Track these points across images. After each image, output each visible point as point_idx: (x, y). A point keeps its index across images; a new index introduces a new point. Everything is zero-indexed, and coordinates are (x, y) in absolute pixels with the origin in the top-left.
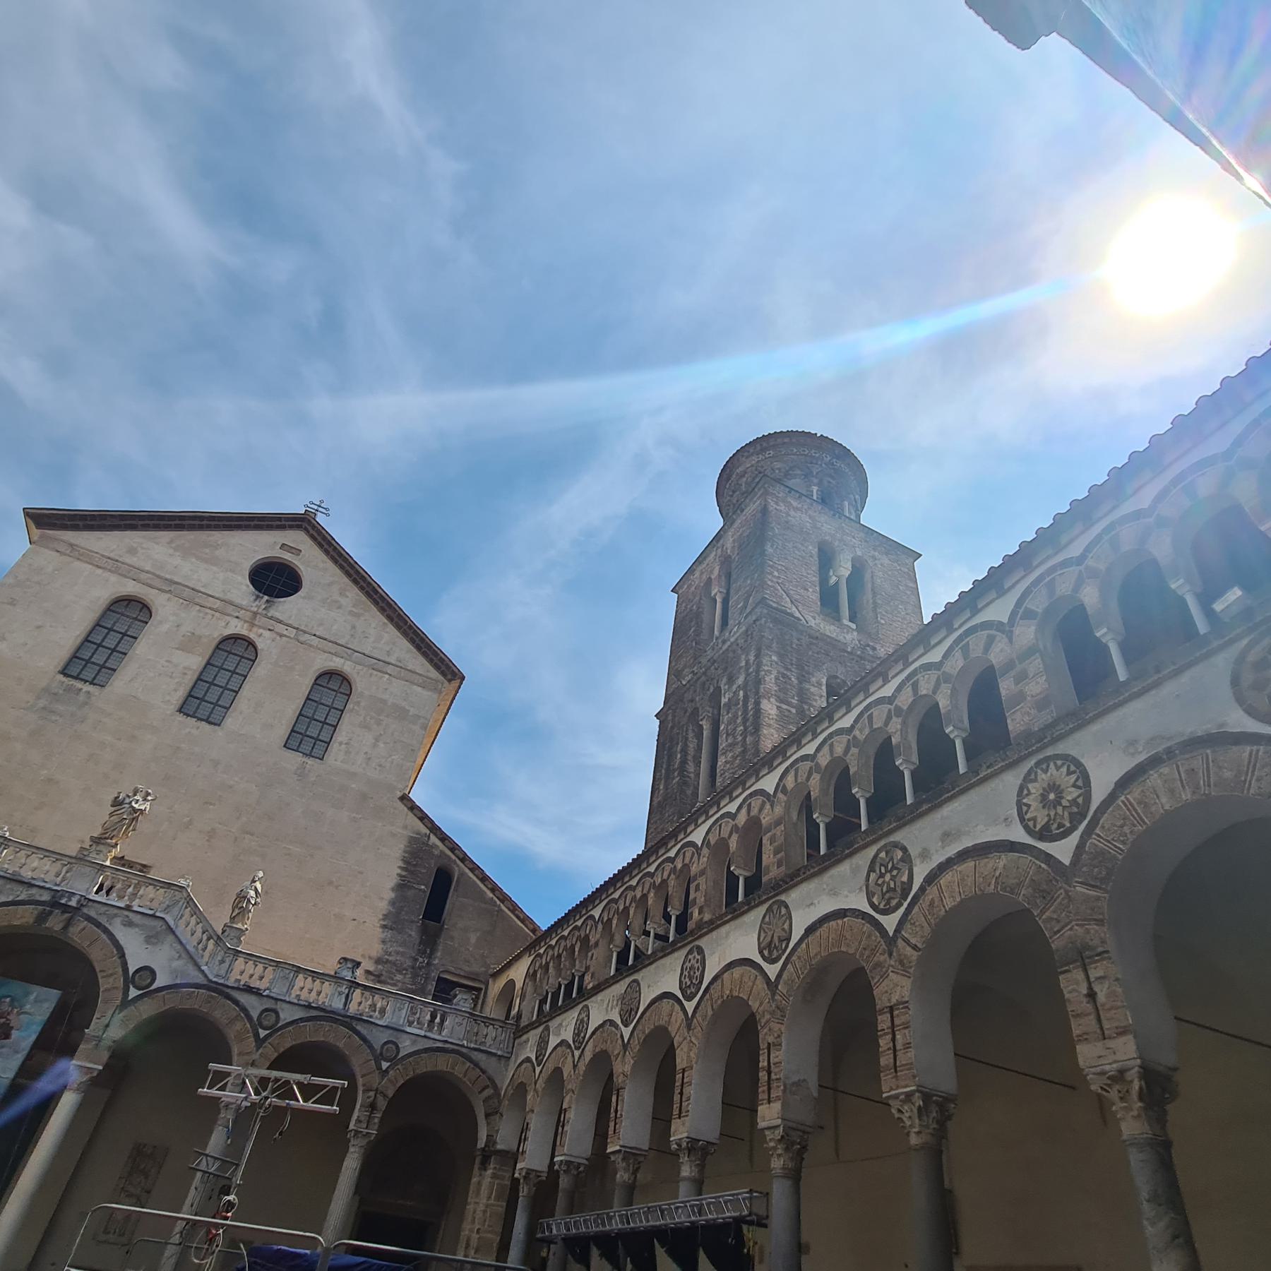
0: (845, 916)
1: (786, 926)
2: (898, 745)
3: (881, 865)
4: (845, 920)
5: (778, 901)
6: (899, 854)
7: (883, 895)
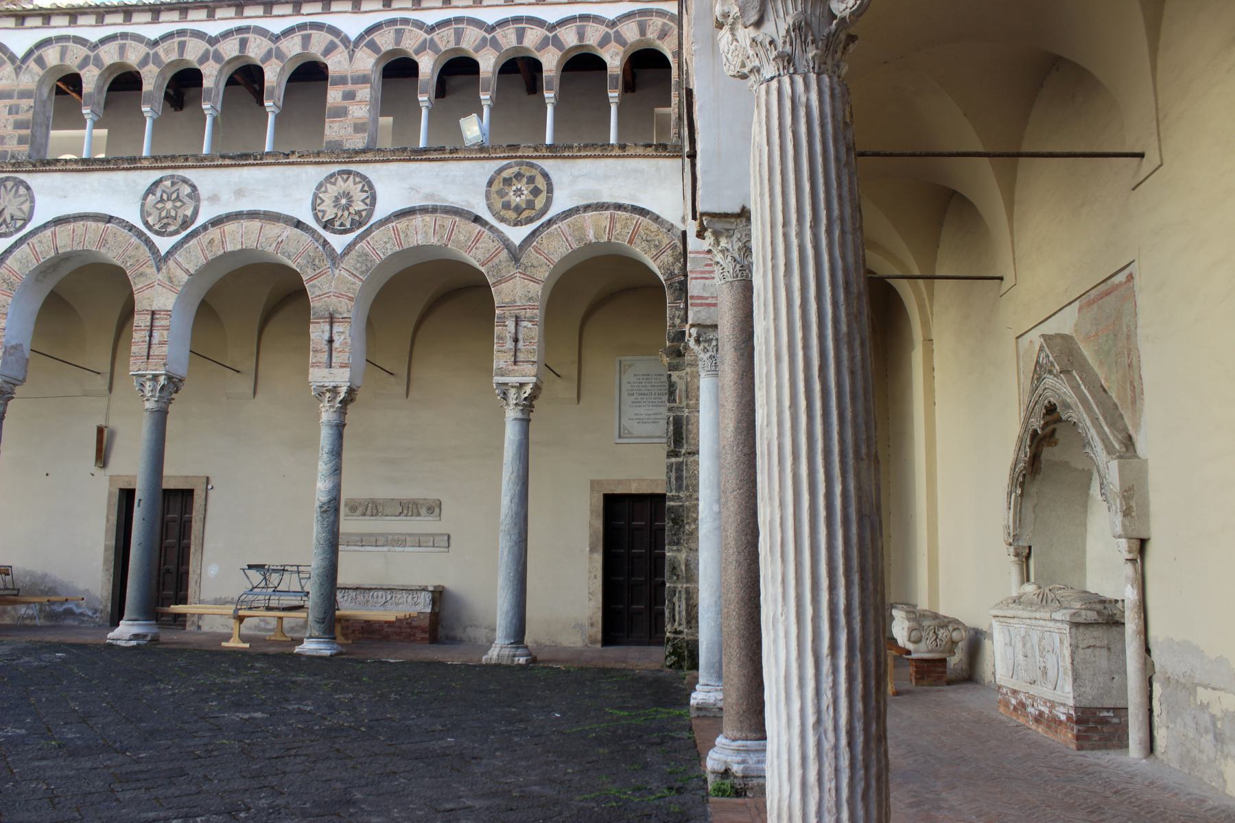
0: (109, 222)
1: (26, 207)
2: (209, 90)
3: (164, 191)
4: (108, 225)
5: (16, 178)
6: (187, 190)
7: (160, 219)
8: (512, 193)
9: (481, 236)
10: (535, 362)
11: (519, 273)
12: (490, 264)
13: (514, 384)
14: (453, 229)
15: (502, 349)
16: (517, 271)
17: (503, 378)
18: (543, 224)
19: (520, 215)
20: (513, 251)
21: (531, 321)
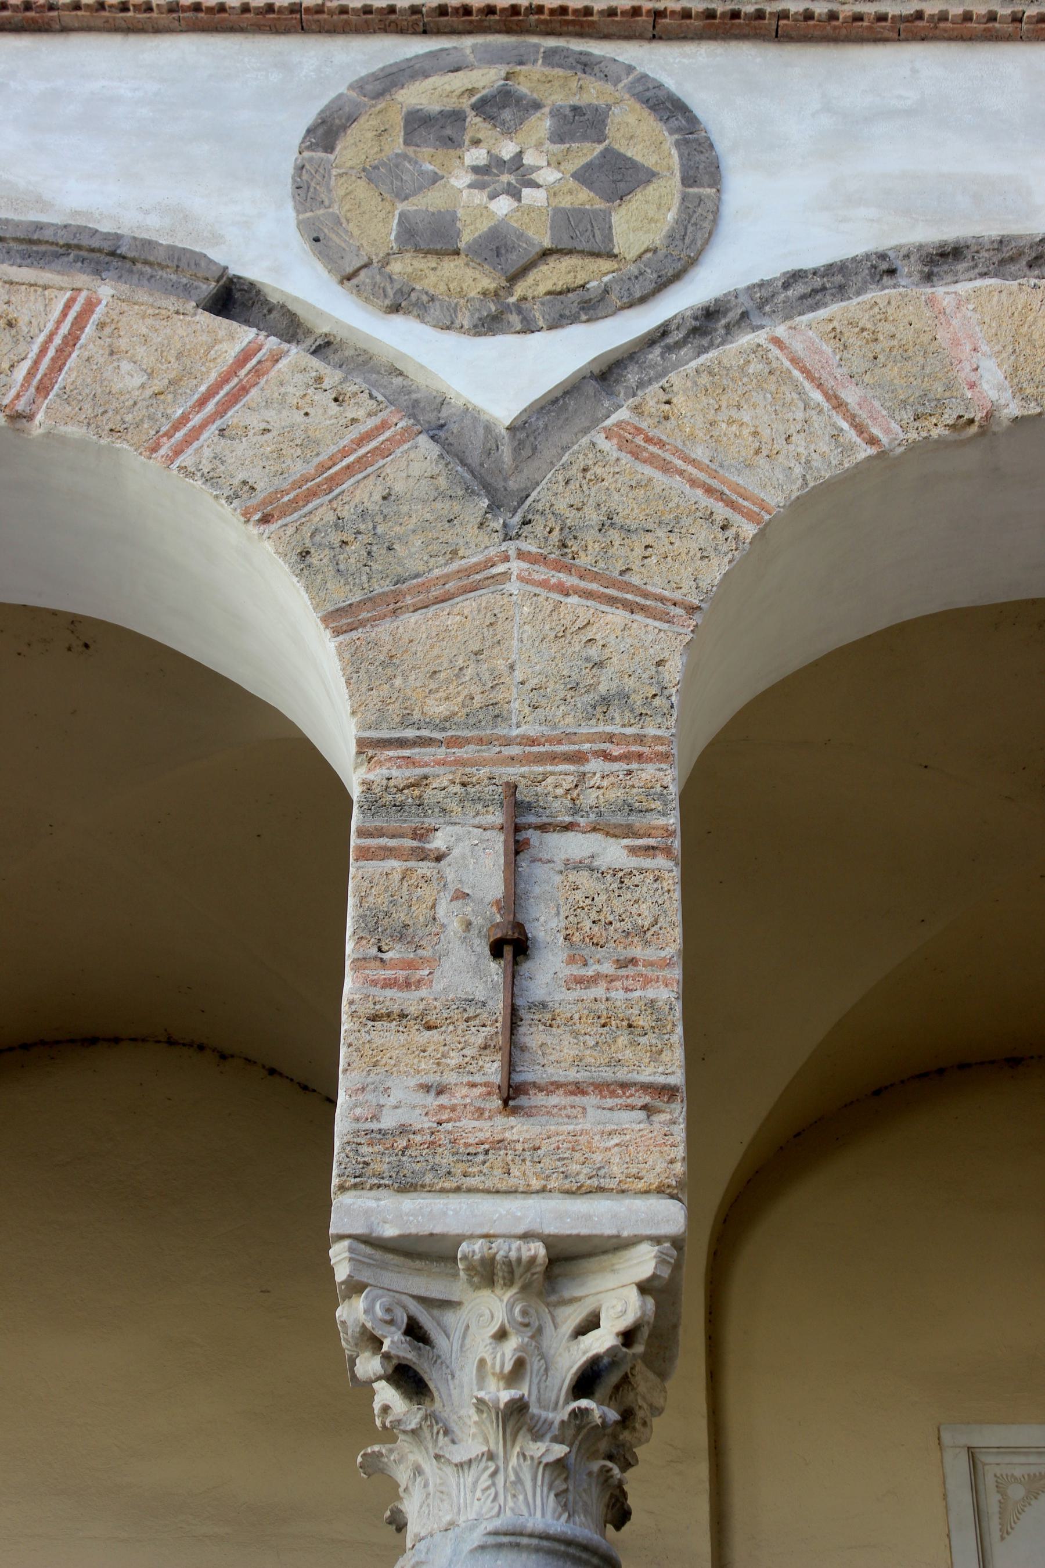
8: (461, 180)
9: (258, 372)
10: (668, 1092)
11: (521, 555)
12: (321, 512)
13: (502, 1249)
14: (72, 340)
15: (410, 1001)
16: (511, 547)
17: (409, 1203)
18: (663, 331)
19: (513, 279)
20: (474, 458)
21: (629, 832)
